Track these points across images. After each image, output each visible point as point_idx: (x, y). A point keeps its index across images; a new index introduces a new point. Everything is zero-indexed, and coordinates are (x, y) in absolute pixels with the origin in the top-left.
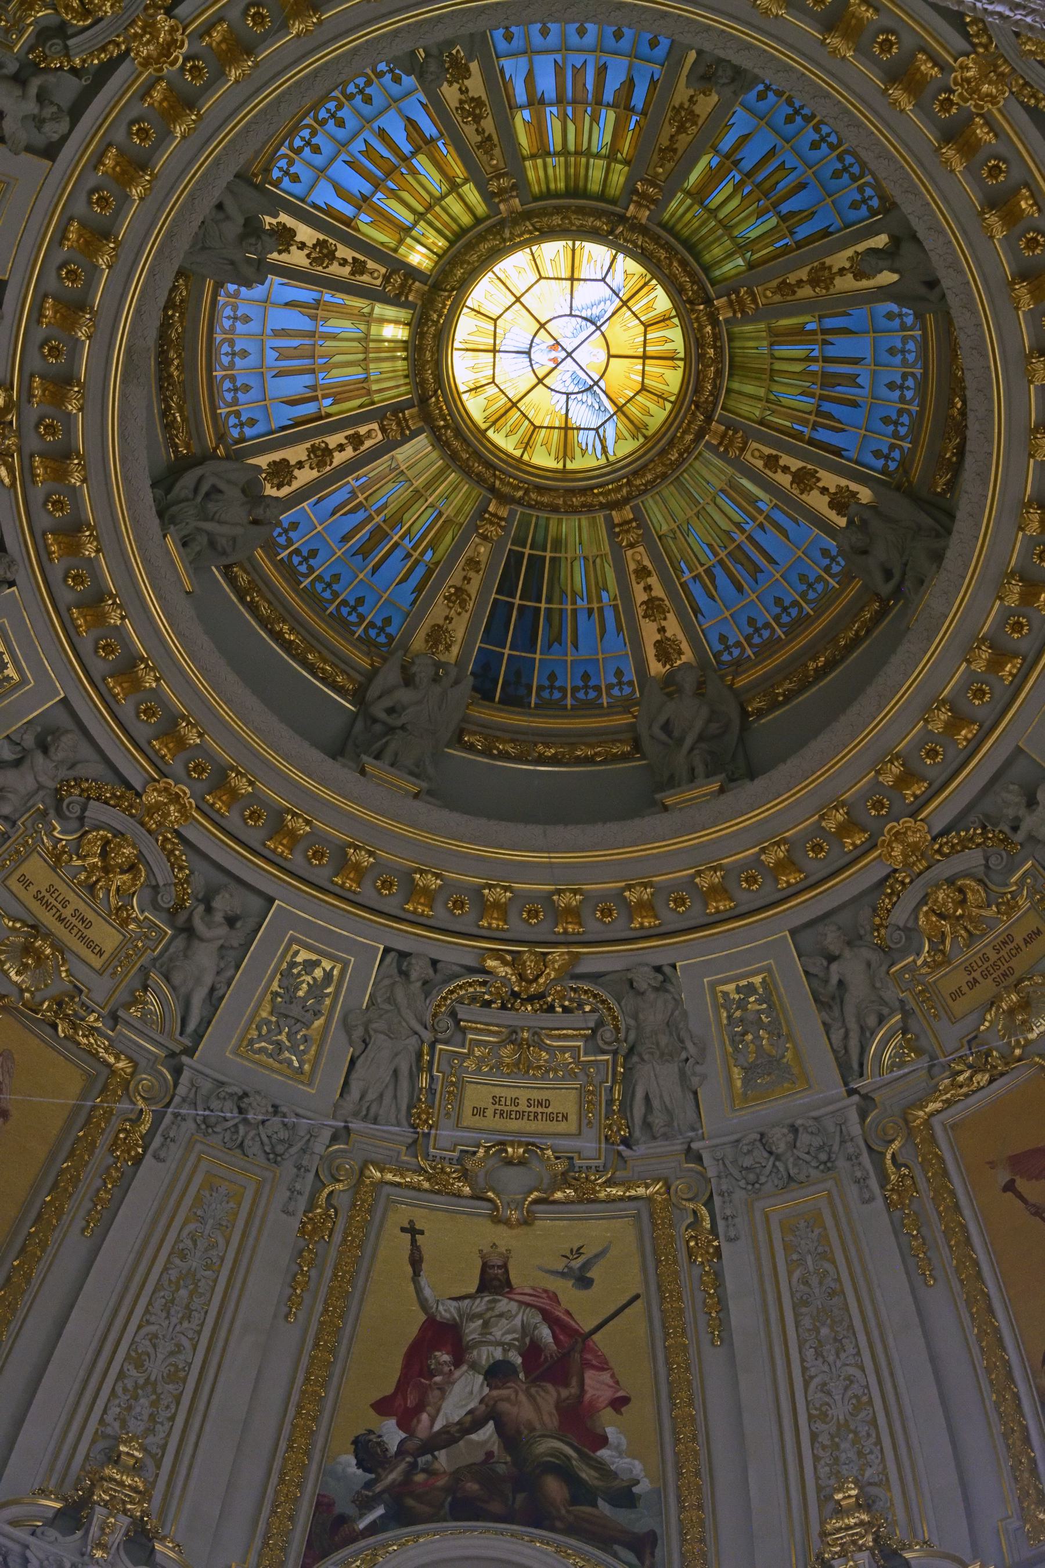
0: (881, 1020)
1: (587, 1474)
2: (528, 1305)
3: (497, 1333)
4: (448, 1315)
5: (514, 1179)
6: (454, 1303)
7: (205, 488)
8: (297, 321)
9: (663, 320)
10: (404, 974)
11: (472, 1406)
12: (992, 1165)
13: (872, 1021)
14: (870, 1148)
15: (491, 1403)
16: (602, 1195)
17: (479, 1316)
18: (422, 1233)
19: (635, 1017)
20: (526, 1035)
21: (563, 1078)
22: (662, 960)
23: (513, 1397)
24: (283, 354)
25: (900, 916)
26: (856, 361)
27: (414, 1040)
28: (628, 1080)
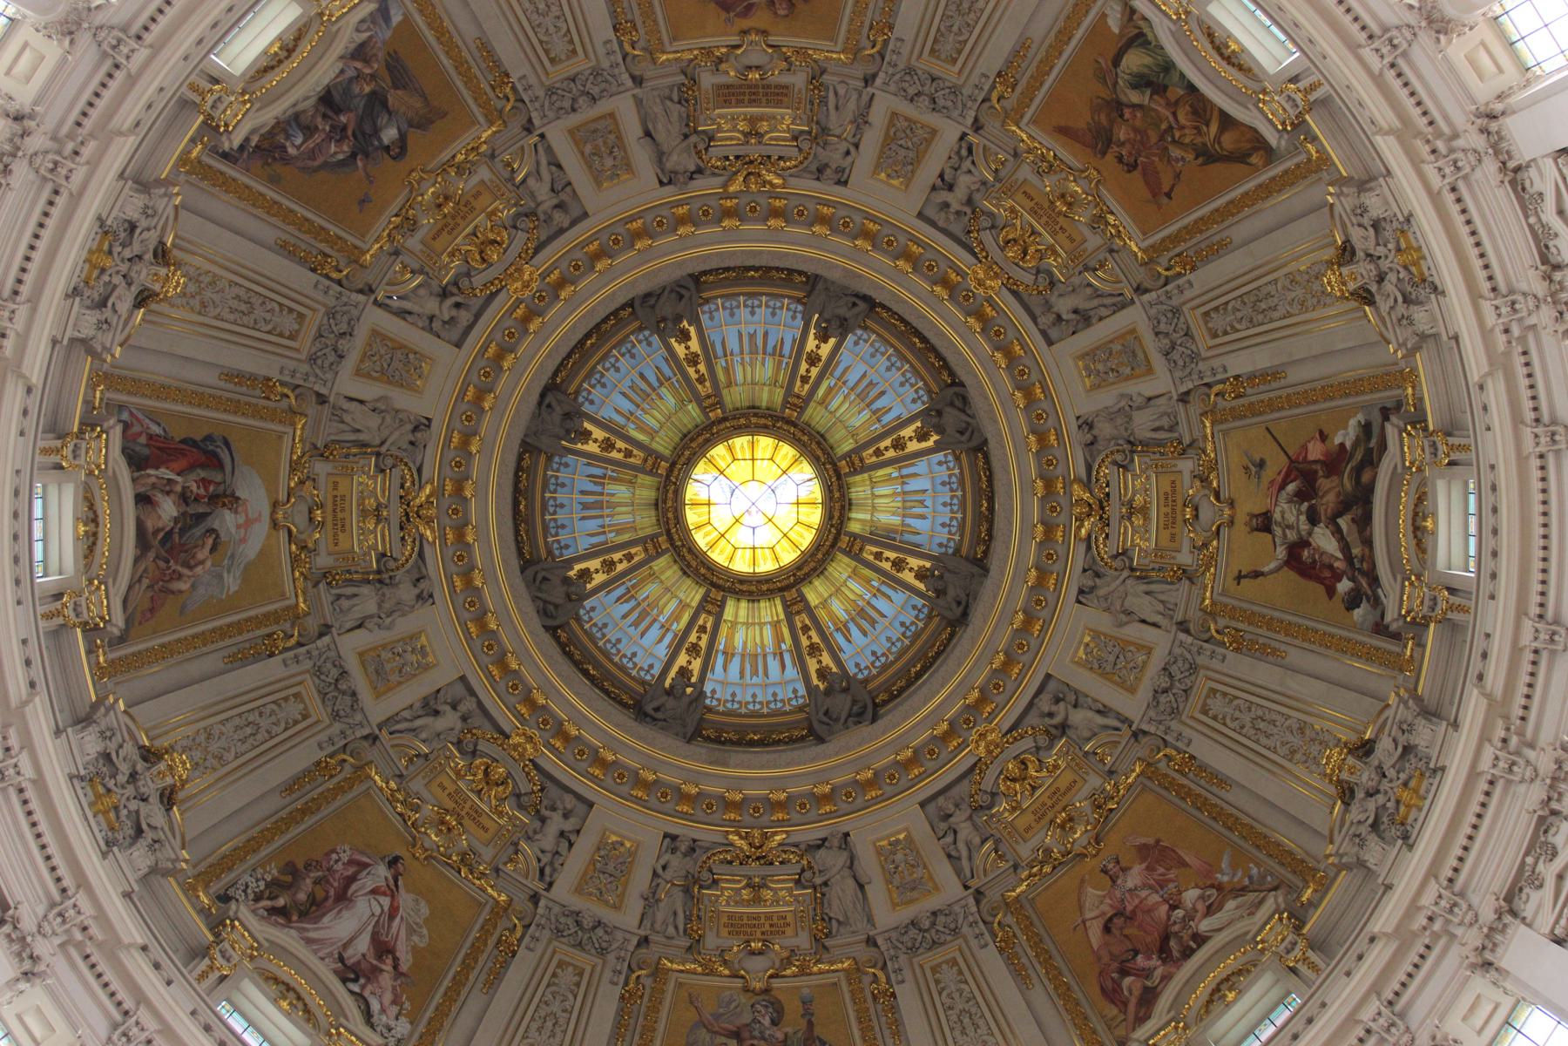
0: (1090, 285)
1: (1358, 456)
3: (1291, 519)
5: (1206, 514)
7: (825, 719)
8: (735, 666)
9: (730, 449)
10: (1093, 589)
12: (1160, 207)
13: (1089, 291)
14: (1165, 284)
22: (1074, 425)
24: (755, 673)
25: (1028, 278)
26: (740, 335)
27: (1129, 582)
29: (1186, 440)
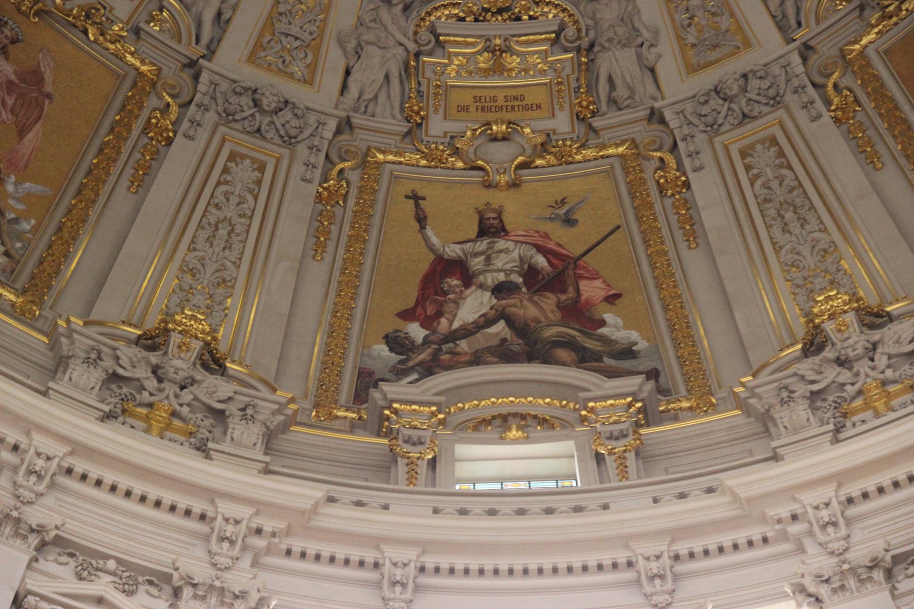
1: (590, 344)
2: (523, 242)
4: (453, 254)
5: (500, 151)
6: (458, 246)
11: (484, 311)
15: (500, 309)
16: (578, 157)
17: (482, 253)
18: (424, 199)
19: (593, 18)
20: (498, 41)
21: (534, 76)
23: (518, 304)
27: (400, 50)
28: (590, 68)
29: (597, 123)
